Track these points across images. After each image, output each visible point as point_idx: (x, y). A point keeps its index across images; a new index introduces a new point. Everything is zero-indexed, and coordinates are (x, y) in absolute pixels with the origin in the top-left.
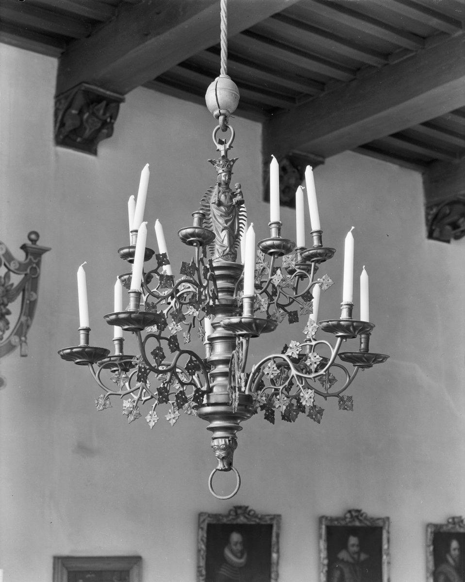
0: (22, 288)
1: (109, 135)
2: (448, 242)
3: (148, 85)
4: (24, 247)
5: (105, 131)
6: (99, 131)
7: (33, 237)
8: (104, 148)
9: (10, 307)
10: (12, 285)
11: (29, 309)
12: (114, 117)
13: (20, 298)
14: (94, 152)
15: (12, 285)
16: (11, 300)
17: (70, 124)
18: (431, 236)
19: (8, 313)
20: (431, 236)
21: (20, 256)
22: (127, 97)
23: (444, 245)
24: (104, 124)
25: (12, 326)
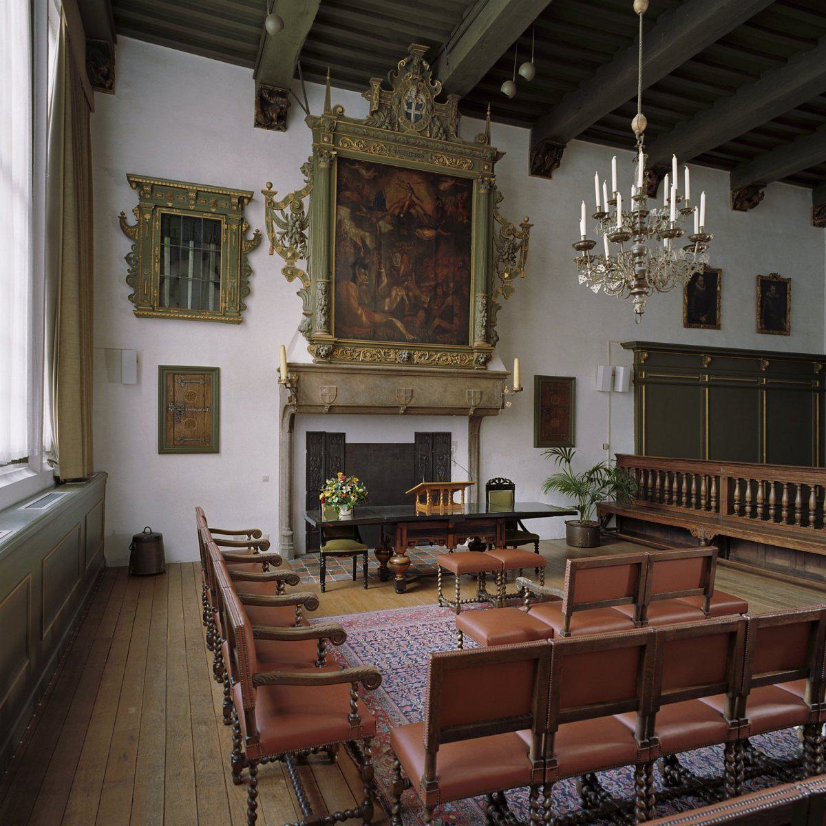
1: (558, 166)
2: (746, 211)
3: (580, 137)
5: (556, 164)
6: (553, 164)
7: (526, 219)
12: (560, 157)
13: (520, 250)
17: (538, 163)
18: (735, 208)
20: (735, 208)
21: (519, 229)
22: (567, 144)
23: (745, 213)
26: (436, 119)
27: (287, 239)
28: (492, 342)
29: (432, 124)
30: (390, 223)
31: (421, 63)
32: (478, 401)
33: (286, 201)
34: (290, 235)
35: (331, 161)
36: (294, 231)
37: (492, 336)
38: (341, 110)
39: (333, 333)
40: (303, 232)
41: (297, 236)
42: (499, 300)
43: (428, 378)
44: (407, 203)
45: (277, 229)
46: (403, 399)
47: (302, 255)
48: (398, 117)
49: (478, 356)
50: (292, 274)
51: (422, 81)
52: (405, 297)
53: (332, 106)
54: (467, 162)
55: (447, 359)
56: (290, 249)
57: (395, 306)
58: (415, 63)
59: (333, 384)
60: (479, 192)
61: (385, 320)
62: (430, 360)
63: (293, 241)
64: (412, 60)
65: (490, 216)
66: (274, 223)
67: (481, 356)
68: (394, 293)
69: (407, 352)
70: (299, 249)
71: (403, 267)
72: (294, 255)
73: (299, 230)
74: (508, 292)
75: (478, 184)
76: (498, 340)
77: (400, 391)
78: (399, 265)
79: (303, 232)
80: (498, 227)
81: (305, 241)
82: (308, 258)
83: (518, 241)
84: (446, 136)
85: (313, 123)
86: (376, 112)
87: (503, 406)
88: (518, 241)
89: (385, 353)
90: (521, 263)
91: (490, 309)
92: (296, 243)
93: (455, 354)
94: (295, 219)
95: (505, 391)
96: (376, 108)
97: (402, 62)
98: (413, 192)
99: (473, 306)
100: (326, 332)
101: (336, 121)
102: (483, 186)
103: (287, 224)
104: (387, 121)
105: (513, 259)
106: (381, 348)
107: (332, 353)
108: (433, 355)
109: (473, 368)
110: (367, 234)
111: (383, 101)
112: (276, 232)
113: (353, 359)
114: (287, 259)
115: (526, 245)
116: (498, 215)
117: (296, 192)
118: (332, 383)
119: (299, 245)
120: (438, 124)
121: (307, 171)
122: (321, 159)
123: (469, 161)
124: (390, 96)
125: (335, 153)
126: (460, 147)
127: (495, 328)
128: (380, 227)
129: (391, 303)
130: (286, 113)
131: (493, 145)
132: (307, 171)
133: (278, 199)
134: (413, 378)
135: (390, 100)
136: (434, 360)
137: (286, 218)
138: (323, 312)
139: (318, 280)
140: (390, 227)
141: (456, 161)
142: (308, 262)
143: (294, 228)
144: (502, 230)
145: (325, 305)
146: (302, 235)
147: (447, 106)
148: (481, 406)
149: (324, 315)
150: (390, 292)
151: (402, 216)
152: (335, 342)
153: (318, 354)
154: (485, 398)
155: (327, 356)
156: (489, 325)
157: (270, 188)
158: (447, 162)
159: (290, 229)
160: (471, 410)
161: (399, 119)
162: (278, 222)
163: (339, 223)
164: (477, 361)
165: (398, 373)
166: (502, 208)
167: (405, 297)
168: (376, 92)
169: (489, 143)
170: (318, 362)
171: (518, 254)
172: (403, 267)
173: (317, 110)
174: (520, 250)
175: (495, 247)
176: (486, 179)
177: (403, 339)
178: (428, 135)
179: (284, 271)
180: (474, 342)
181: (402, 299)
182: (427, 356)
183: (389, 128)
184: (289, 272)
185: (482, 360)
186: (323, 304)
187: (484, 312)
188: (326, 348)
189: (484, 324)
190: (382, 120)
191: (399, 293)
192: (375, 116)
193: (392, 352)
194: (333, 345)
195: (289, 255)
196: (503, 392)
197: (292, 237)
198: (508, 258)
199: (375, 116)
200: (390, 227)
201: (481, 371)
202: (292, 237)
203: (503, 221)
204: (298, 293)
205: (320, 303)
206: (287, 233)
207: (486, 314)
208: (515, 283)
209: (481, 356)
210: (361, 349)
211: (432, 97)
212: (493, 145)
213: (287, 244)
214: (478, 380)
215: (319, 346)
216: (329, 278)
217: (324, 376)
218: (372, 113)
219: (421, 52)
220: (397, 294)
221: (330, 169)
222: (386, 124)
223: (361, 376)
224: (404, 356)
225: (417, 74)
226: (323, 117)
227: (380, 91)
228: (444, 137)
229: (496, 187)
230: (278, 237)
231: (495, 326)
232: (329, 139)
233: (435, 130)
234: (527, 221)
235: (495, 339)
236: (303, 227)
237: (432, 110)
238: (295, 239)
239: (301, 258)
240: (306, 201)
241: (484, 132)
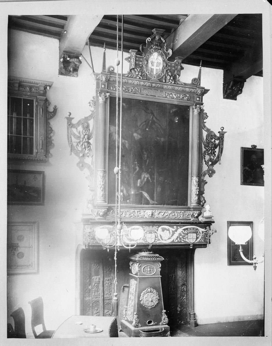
0: (219, 144)
1: (241, 93)
4: (219, 132)
5: (240, 92)
6: (238, 92)
7: (222, 129)
8: (238, 97)
9: (216, 150)
10: (216, 144)
11: (221, 151)
12: (242, 87)
13: (218, 147)
14: (236, 100)
15: (216, 144)
16: (216, 148)
19: (215, 152)
21: (218, 135)
24: (239, 90)
25: (216, 155)
26: (168, 71)
27: (79, 145)
28: (201, 203)
29: (166, 75)
30: (140, 135)
31: (160, 39)
33: (79, 123)
34: (81, 143)
35: (106, 99)
36: (84, 141)
37: (202, 200)
38: (113, 69)
39: (107, 202)
40: (89, 141)
41: (86, 144)
42: (207, 178)
44: (150, 122)
45: (74, 140)
47: (88, 155)
48: (146, 71)
50: (82, 166)
51: (160, 49)
52: (149, 178)
53: (107, 66)
54: (186, 96)
56: (81, 152)
57: (143, 183)
58: (157, 38)
60: (193, 113)
61: (137, 193)
62: (165, 215)
63: (83, 146)
64: (155, 37)
65: (201, 126)
66: (72, 136)
67: (195, 213)
68: (143, 176)
70: (87, 151)
71: (148, 161)
72: (84, 155)
73: (87, 140)
74: (211, 173)
75: (193, 109)
76: (205, 202)
78: (146, 159)
79: (89, 141)
80: (205, 134)
81: (90, 146)
82: (92, 156)
83: (217, 142)
84: (174, 81)
85: (96, 75)
86: (133, 69)
87: (210, 243)
88: (217, 142)
90: (219, 155)
91: (201, 184)
92: (85, 148)
93: (179, 211)
94: (84, 134)
96: (133, 67)
97: (149, 39)
98: (154, 115)
99: (190, 185)
100: (104, 201)
101: (109, 76)
102: (196, 110)
103: (79, 137)
104: (140, 74)
105: (214, 153)
107: (106, 213)
110: (126, 141)
111: (137, 62)
112: (73, 141)
114: (80, 158)
115: (223, 144)
116: (205, 126)
117: (85, 118)
119: (87, 149)
120: (170, 74)
121: (92, 104)
122: (100, 98)
123: (188, 95)
124: (141, 59)
125: (109, 94)
126: (182, 87)
127: (203, 195)
128: (134, 137)
129: (141, 182)
130: (78, 68)
131: (202, 85)
132: (92, 104)
133: (74, 122)
135: (141, 61)
137: (79, 133)
138: (102, 189)
139: (99, 170)
140: (139, 137)
141: (180, 96)
142: (92, 159)
143: (84, 139)
144: (207, 136)
145: (103, 185)
146: (89, 143)
147: (175, 63)
149: (102, 190)
150: (141, 175)
151: (147, 129)
152: (109, 207)
155: (103, 216)
156: (201, 193)
157: (70, 115)
158: (175, 97)
159: (81, 140)
161: (147, 73)
162: (74, 135)
163: (111, 135)
166: (209, 123)
167: (149, 178)
168: (133, 57)
169: (200, 84)
171: (217, 150)
172: (148, 161)
173: (99, 69)
174: (218, 147)
175: (203, 146)
176: (198, 106)
177: (148, 203)
178: (164, 81)
179: (78, 164)
180: (191, 203)
181: (148, 178)
182: (163, 214)
183: (141, 78)
184: (81, 165)
185: (196, 215)
186: (102, 183)
187: (197, 186)
188: (104, 211)
189: (197, 193)
190: (137, 73)
191: (146, 176)
192: (133, 71)
193: (142, 211)
194: (107, 209)
195: (81, 155)
197: (83, 144)
198: (211, 153)
199: (133, 71)
200: (139, 137)
202: (83, 144)
203: (208, 130)
204: (86, 177)
205: (99, 183)
206: (80, 142)
207: (198, 188)
208: (216, 167)
209: (195, 213)
211: (166, 58)
212: (202, 85)
213: (80, 148)
215: (99, 209)
216: (105, 169)
218: (131, 70)
219: (161, 33)
220: (144, 177)
221: (105, 102)
222: (139, 76)
224: (149, 214)
225: (157, 45)
226: (102, 73)
227: (136, 57)
228: (173, 82)
229: (204, 110)
230: (75, 144)
231: (204, 193)
232: (105, 85)
233: (168, 77)
234: (223, 130)
235: (203, 202)
236: (89, 138)
237: (166, 66)
238: (85, 145)
239: (88, 156)
240: (91, 122)
241: (197, 77)
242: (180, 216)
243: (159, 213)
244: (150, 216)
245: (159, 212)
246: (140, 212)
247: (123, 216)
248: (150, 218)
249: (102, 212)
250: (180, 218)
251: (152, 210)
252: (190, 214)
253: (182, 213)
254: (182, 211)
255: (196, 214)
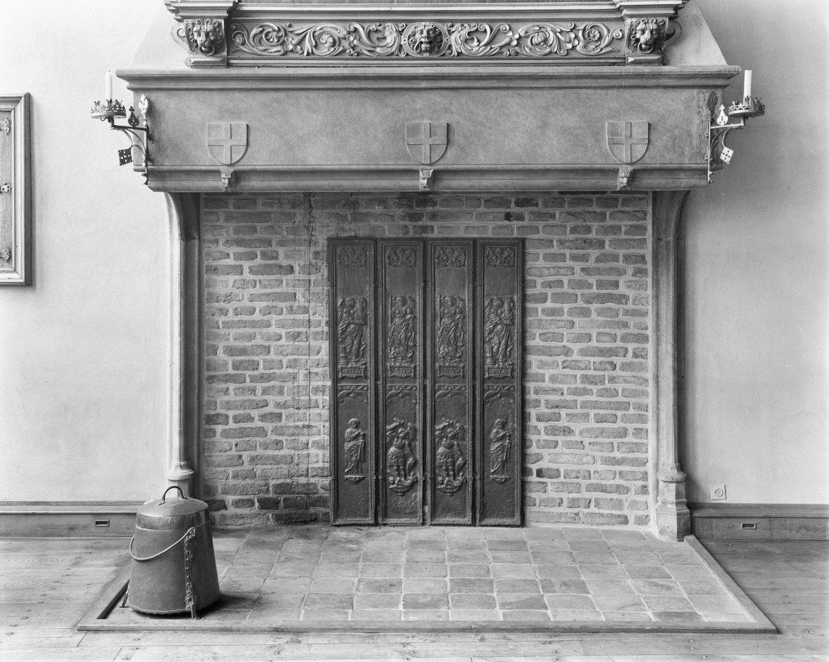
32: (640, 150)
43: (492, 94)
46: (425, 150)
49: (632, 30)
55: (545, 40)
59: (240, 118)
62: (496, 46)
67: (641, 26)
69: (429, 26)
77: (414, 130)
89: (369, 34)
93: (567, 27)
95: (719, 120)
106: (358, 21)
108: (505, 32)
109: (623, 62)
113: (286, 53)
118: (235, 114)
134: (453, 94)
136: (509, 44)
148: (650, 162)
153: (193, 45)
154: (661, 140)
155: (213, 46)
160: (622, 174)
164: (633, 41)
165: (405, 85)
170: (197, 65)
185: (644, 38)
188: (209, 27)
196: (713, 122)
201: (647, 69)
210: (304, 27)
214: (639, 92)
217: (218, 98)
223: (312, 95)
242: (570, 46)
243: (469, 33)
244: (423, 46)
245: (465, 32)
246: (379, 35)
247: (305, 53)
248: (426, 55)
249: (202, 34)
250: (573, 54)
251: (439, 25)
252: (617, 34)
253: (580, 34)
254: (581, 26)
255: (643, 32)
